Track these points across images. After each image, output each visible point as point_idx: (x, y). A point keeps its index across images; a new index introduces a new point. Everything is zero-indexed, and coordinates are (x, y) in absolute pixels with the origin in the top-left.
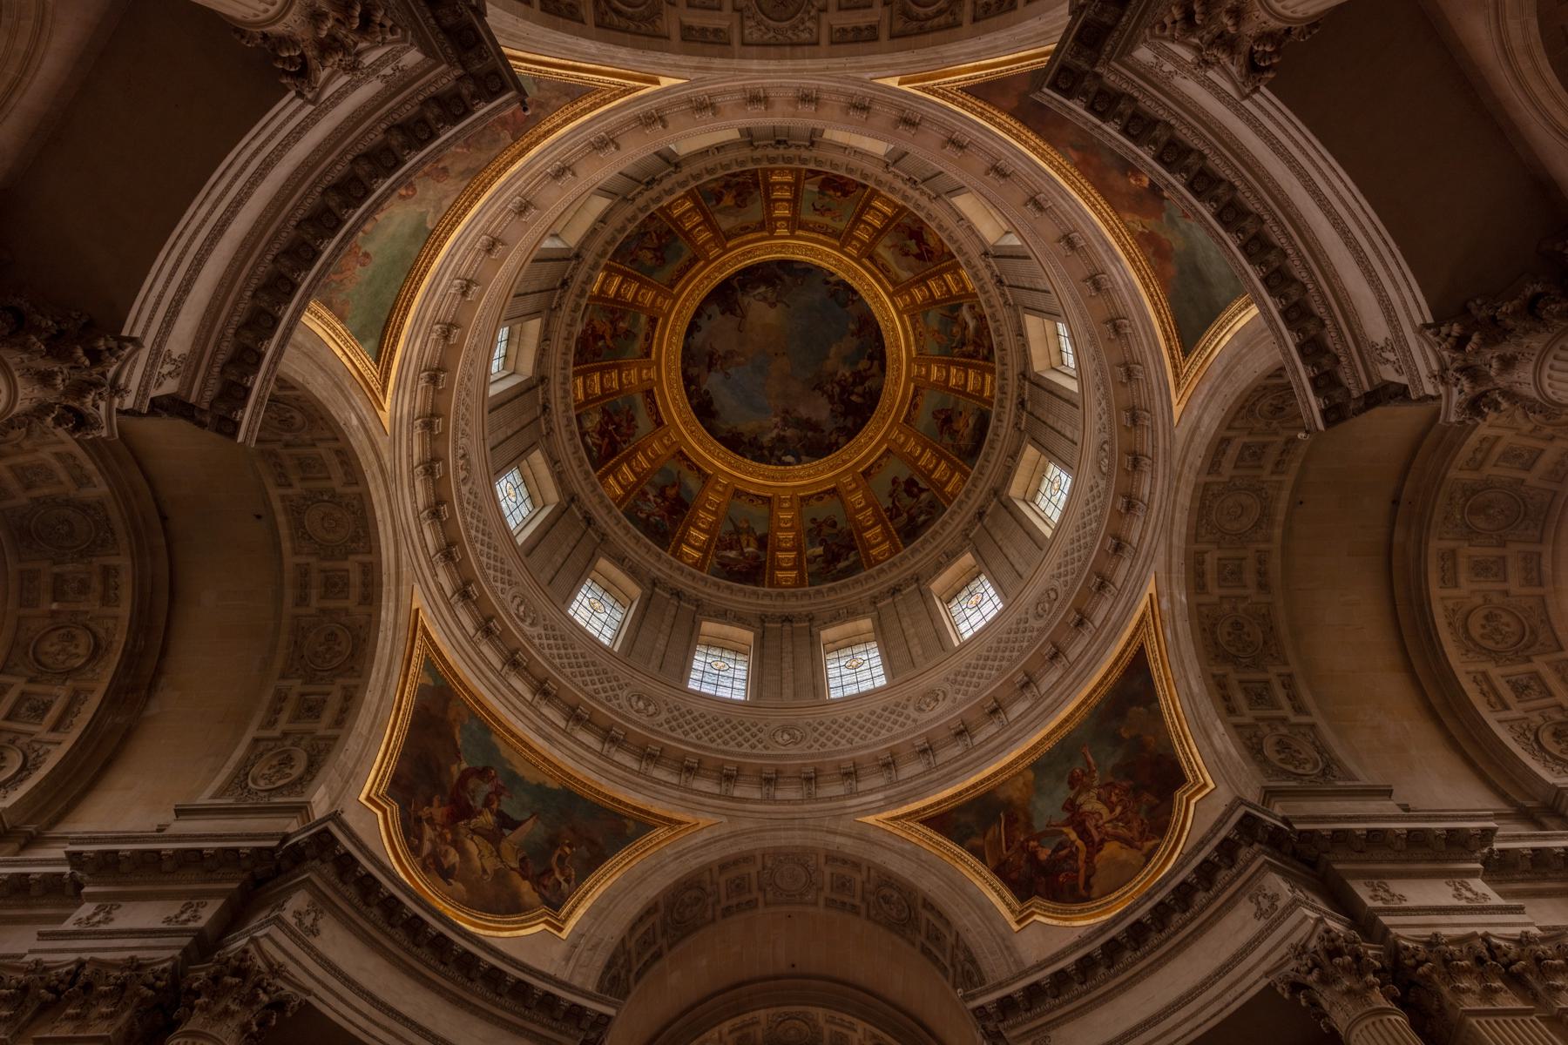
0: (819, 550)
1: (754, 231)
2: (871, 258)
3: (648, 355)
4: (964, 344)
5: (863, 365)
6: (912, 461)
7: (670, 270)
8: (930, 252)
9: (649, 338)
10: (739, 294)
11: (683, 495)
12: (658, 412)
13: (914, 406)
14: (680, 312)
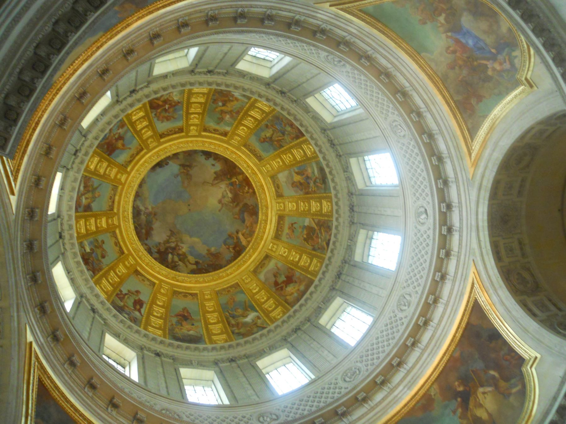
0: (88, 250)
1: (276, 191)
2: (267, 257)
3: (205, 130)
4: (233, 317)
5: (191, 259)
6: (153, 302)
7: (257, 146)
8: (282, 288)
9: (215, 131)
10: (228, 182)
11: (117, 152)
12: (169, 135)
13: (185, 295)
14: (227, 148)
